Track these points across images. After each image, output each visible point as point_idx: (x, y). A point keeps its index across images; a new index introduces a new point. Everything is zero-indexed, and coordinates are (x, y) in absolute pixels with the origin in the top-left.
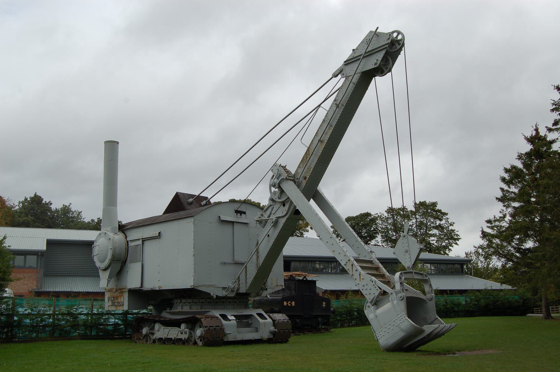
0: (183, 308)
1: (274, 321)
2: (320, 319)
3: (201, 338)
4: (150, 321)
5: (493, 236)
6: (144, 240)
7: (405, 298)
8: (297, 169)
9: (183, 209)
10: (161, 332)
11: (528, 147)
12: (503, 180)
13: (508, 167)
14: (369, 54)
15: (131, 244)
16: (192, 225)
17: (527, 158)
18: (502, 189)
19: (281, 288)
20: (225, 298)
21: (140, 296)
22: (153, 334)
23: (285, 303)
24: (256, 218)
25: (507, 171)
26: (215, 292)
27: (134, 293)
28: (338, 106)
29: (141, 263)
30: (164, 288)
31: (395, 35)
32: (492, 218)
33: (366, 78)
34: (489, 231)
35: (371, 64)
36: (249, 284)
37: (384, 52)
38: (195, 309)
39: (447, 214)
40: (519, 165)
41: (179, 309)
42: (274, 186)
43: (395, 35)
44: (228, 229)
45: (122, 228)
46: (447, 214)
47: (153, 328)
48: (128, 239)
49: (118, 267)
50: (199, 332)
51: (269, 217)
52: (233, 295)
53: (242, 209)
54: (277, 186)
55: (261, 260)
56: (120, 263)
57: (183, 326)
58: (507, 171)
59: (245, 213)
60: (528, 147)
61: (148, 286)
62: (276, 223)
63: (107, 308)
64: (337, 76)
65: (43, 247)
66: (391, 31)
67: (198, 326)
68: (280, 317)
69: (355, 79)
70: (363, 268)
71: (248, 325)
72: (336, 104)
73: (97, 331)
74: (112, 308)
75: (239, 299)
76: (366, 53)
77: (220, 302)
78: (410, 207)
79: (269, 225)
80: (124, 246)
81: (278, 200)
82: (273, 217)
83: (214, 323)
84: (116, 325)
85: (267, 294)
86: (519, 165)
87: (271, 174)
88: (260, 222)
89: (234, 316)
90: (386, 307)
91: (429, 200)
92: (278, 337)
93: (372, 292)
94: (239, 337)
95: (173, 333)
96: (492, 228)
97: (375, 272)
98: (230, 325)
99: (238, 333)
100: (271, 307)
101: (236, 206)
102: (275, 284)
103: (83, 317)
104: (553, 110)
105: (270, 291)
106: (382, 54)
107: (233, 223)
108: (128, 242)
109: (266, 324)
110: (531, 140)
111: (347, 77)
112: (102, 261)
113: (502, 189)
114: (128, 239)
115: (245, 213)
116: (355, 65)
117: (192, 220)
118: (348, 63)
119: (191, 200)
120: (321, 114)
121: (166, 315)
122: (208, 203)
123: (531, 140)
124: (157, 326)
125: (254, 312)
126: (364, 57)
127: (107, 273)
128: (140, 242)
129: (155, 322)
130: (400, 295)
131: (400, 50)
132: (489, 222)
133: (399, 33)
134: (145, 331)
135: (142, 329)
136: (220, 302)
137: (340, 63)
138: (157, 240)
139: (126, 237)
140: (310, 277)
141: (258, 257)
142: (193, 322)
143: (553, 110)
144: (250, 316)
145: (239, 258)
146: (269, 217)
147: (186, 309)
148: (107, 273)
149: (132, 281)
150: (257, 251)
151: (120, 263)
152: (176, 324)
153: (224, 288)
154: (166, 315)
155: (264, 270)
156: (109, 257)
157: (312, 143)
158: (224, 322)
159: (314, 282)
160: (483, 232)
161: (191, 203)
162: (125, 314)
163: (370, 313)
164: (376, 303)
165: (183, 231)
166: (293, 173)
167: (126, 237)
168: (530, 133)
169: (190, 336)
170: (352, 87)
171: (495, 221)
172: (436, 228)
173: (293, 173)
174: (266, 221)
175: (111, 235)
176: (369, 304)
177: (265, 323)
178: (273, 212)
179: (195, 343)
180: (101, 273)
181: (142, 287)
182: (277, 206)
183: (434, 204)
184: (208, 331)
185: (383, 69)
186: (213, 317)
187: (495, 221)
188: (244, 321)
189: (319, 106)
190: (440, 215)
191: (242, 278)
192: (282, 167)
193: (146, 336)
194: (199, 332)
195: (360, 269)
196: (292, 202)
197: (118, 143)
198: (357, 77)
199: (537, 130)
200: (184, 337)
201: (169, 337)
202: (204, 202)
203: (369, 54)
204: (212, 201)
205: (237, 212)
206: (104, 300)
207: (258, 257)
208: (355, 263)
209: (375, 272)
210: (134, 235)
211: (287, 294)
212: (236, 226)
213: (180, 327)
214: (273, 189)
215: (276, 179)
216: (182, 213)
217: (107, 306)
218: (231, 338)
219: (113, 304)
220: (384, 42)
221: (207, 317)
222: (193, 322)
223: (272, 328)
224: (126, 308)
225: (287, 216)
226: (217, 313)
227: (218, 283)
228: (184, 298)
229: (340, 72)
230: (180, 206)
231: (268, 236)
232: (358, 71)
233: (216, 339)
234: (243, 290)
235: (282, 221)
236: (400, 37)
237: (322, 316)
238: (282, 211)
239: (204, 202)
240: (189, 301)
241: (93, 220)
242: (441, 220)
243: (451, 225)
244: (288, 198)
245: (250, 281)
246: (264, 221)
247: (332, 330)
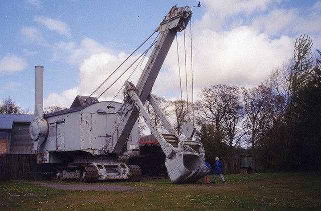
0: (79, 161)
6: (57, 123)
7: (183, 156)
10: (67, 175)
37: (179, 19)
43: (187, 8)
47: (62, 173)
49: (43, 139)
57: (77, 171)
64: (157, 31)
67: (84, 172)
77: (96, 158)
82: (126, 111)
83: (91, 169)
112: (34, 136)
126: (170, 21)
128: (55, 124)
134: (58, 175)
136: (96, 158)
142: (81, 169)
144: (117, 166)
149: (51, 146)
152: (73, 170)
169: (81, 177)
191: (110, 144)
194: (84, 175)
197: (43, 67)
200: (78, 177)
213: (75, 172)
226: (95, 164)
234: (111, 151)
235: (130, 113)
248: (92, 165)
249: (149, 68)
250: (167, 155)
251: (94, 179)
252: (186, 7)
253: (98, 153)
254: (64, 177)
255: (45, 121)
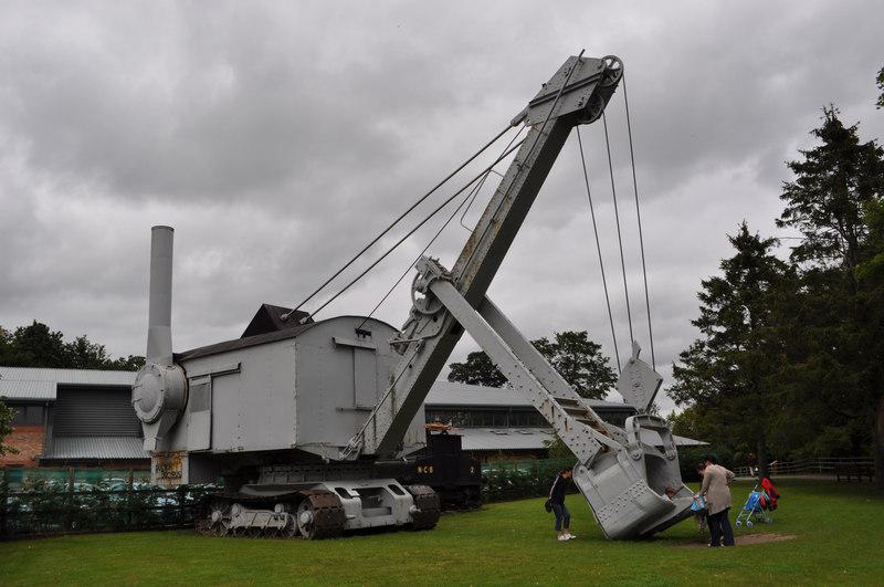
0: (277, 480)
1: (415, 496)
2: (468, 492)
3: (308, 526)
4: (226, 502)
5: (691, 373)
6: (214, 376)
8: (456, 265)
9: (274, 329)
10: (242, 517)
11: (734, 252)
12: (703, 297)
13: (708, 280)
14: (568, 91)
15: (192, 383)
16: (292, 351)
17: (733, 266)
18: (703, 309)
19: (422, 446)
20: (344, 462)
21: (204, 461)
22: (229, 521)
23: (420, 470)
24: (391, 340)
25: (705, 284)
26: (328, 455)
27: (199, 459)
28: (521, 169)
29: (209, 411)
30: (248, 448)
31: (609, 62)
32: (688, 349)
33: (564, 125)
34: (683, 366)
35: (572, 105)
36: (379, 441)
37: (593, 87)
38: (295, 480)
39: (599, 347)
40: (722, 275)
41: (269, 481)
42: (420, 291)
44: (346, 358)
45: (178, 360)
46: (599, 347)
47: (228, 512)
48: (188, 376)
50: (305, 517)
51: (411, 337)
52: (355, 458)
53: (366, 328)
54: (425, 290)
55: (399, 405)
56: (174, 413)
57: (278, 508)
58: (705, 284)
59: (369, 334)
60: (734, 252)
61: (220, 446)
62: (422, 348)
63: (153, 483)
65: (53, 395)
66: (600, 57)
67: (301, 508)
68: (422, 490)
69: (549, 128)
70: (566, 410)
71: (377, 504)
72: (519, 165)
73: (136, 517)
74: (163, 485)
75: (361, 466)
76: (565, 88)
77: (336, 470)
78: (553, 341)
79: (411, 353)
80: (182, 386)
81: (425, 312)
82: (418, 338)
83: (328, 502)
84: (168, 507)
85: (403, 456)
86: (722, 275)
87: (414, 272)
88: (396, 346)
89: (357, 490)
90: (610, 472)
91: (577, 330)
92: (421, 522)
93: (588, 448)
94: (366, 523)
95: (263, 519)
96: (687, 362)
97: (583, 419)
98: (352, 502)
99: (365, 516)
100: (407, 476)
101: (357, 324)
102: (413, 441)
103: (115, 498)
104: (783, 197)
105: (407, 451)
106: (588, 91)
107: (352, 348)
108: (188, 380)
109: (402, 503)
110: (738, 242)
111: (534, 126)
112: (147, 410)
113: (703, 309)
114: (188, 376)
115: (369, 334)
116: (547, 108)
117: (291, 343)
118: (534, 104)
119: (285, 316)
120: (493, 182)
121: (246, 491)
122: (310, 320)
123: (738, 242)
124: (235, 509)
125: (384, 484)
126: (562, 94)
127: (156, 427)
128: (208, 379)
129: (232, 502)
130: (635, 452)
131: (615, 85)
132: (684, 354)
133: (614, 59)
134: (216, 516)
135: (211, 514)
136: (336, 470)
137: (522, 105)
138: (236, 376)
139: (185, 373)
140: (453, 432)
141: (394, 400)
143: (783, 197)
144: (379, 490)
145: (364, 402)
146: (411, 337)
147: (281, 481)
148: (156, 427)
149: (194, 437)
150: (393, 391)
151: (174, 413)
152: (267, 504)
153: (341, 448)
154: (246, 491)
155: (402, 420)
156: (159, 403)
157: (479, 224)
158: (343, 500)
159: (458, 439)
160: (675, 368)
161: (286, 320)
162: (183, 490)
163: (583, 480)
164: (594, 465)
165: (279, 359)
166: (449, 269)
167: (185, 373)
168: (736, 233)
169: (290, 524)
170: (543, 140)
171: (692, 353)
172: (587, 366)
173: (449, 269)
174: (406, 346)
175: (162, 369)
176: (581, 468)
177: (401, 501)
178: (418, 330)
179: (298, 534)
180: (145, 429)
181: (211, 448)
182: (422, 322)
183: (583, 335)
184: (322, 514)
185: (588, 114)
186: (328, 493)
187: (692, 353)
188: (370, 498)
189: (490, 168)
190: (592, 348)
191: (369, 432)
192: (434, 261)
193: (218, 524)
194: (305, 517)
195: (565, 413)
196: (449, 313)
197: (173, 230)
198: (551, 125)
199: (745, 229)
200: (281, 524)
201: (255, 525)
202: (305, 319)
203: (568, 91)
204: (316, 319)
205: (359, 332)
206: (150, 470)
207: (394, 400)
208: (556, 404)
209: (583, 419)
210: (195, 369)
211: (422, 457)
212: (358, 354)
214: (420, 296)
215: (424, 280)
216: (274, 334)
217: (155, 479)
218: (353, 525)
219: (165, 477)
220: (589, 72)
221: (318, 493)
222: (294, 502)
223: (413, 508)
224: (185, 481)
225: (441, 336)
226: (331, 487)
227: (334, 440)
228: (279, 464)
229: (523, 117)
230: (269, 325)
231: (411, 367)
232: (552, 115)
233: (332, 527)
234: (370, 449)
236: (616, 66)
237: (470, 487)
238: (432, 328)
239: (305, 319)
240: (289, 468)
241: (122, 359)
242: (592, 355)
243: (605, 361)
244: (444, 308)
245: (380, 437)
246: (402, 346)
247: (484, 506)
248: (320, 488)
249: (493, 222)
250: (583, 457)
251: (332, 527)
252: (607, 58)
253: (342, 456)
254: (235, 523)
255: (177, 370)
